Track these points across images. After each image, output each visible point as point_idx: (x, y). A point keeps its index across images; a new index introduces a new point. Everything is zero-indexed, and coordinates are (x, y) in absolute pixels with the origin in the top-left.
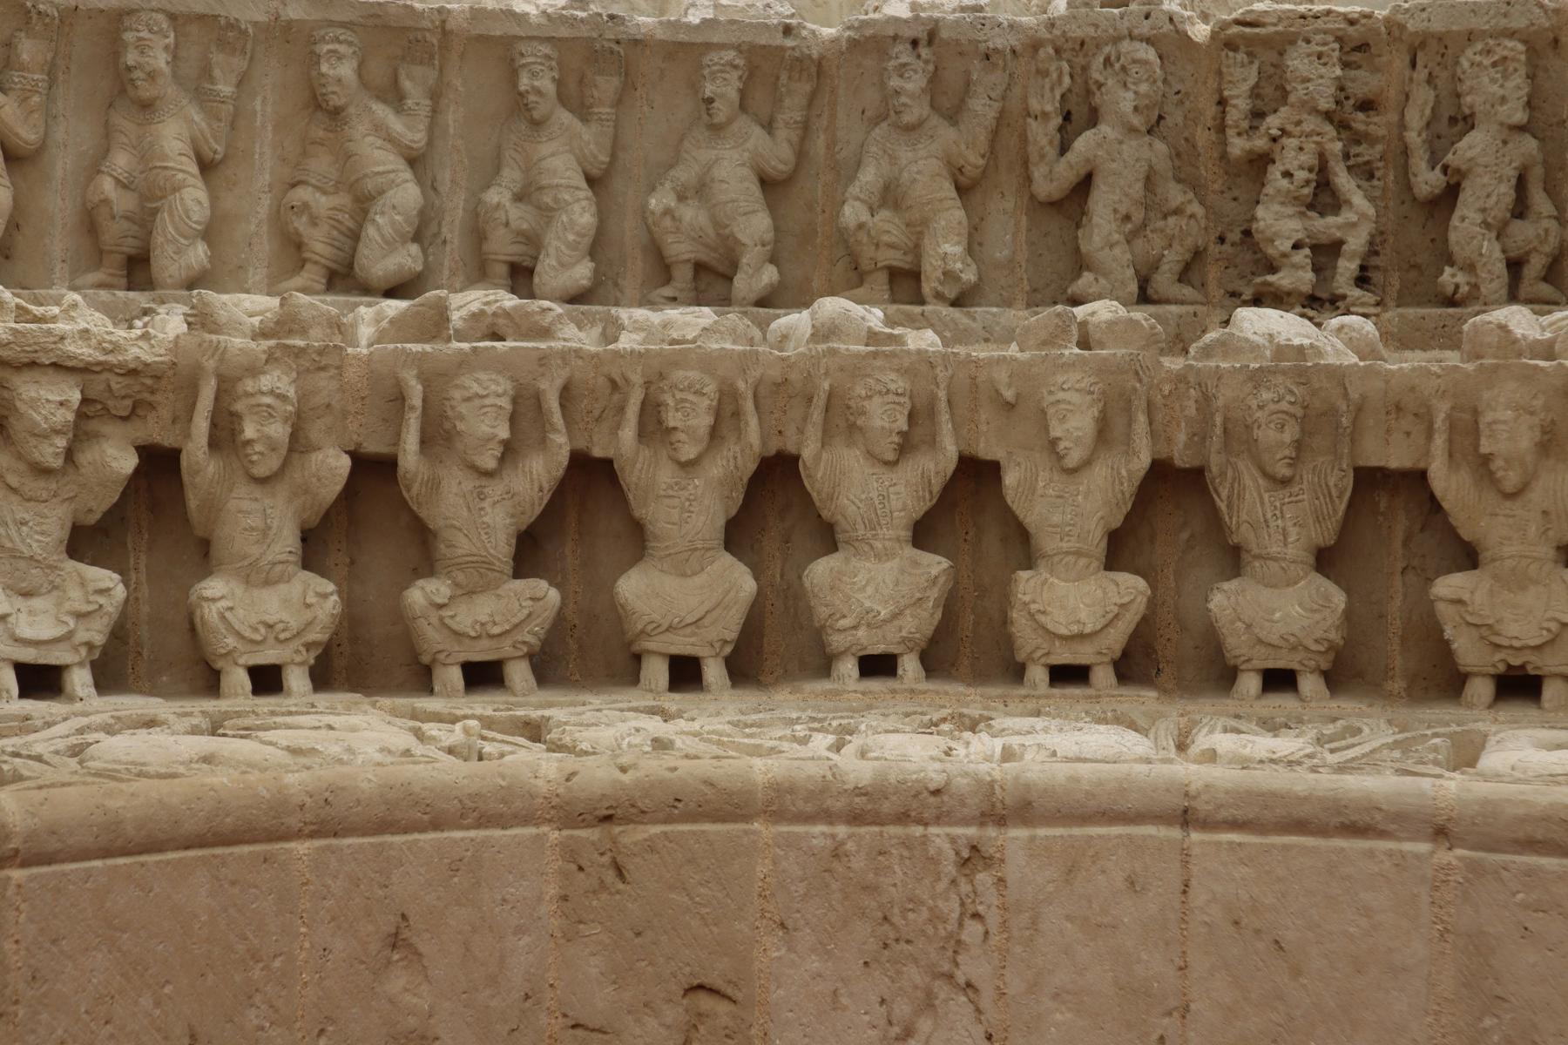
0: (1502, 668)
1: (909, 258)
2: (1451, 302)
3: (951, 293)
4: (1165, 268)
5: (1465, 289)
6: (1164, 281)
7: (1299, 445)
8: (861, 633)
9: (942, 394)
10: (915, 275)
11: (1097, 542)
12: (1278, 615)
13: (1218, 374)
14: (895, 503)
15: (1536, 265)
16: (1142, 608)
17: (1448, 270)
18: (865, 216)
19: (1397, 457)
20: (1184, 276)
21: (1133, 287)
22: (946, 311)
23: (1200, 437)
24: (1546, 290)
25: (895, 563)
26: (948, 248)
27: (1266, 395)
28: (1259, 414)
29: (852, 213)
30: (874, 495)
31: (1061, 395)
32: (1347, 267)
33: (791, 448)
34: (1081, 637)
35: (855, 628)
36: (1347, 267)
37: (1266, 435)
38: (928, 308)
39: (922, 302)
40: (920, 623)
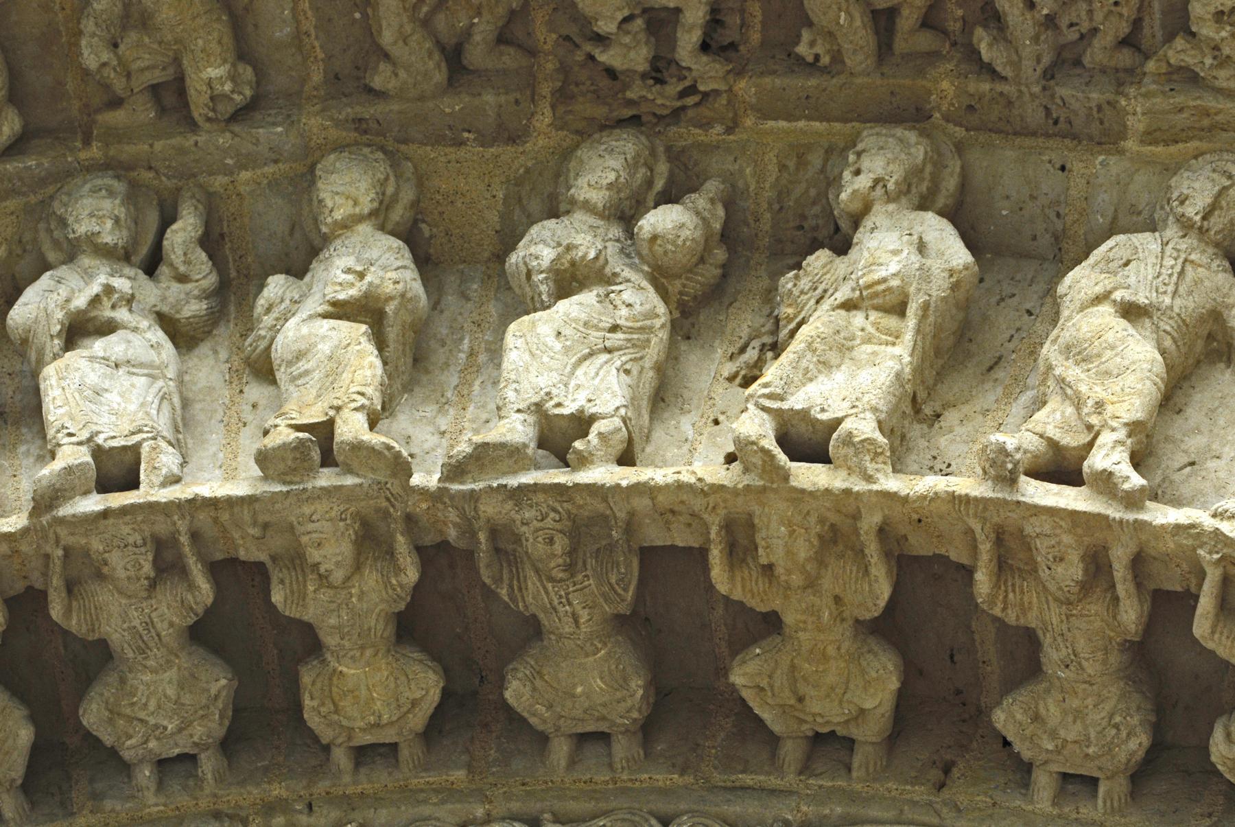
0: (810, 734)
1: (171, 70)
2: (813, 66)
3: (226, 109)
4: (478, 38)
5: (825, 60)
6: (476, 55)
7: (572, 552)
8: (152, 744)
9: (184, 539)
10: (179, 85)
11: (380, 628)
12: (579, 690)
13: (473, 496)
14: (162, 627)
15: (908, 20)
16: (437, 698)
17: (806, 35)
18: (105, 56)
19: (681, 538)
20: (503, 39)
21: (440, 77)
22: (224, 140)
23: (469, 531)
24: (925, 41)
25: (172, 674)
26: (213, 72)
27: (528, 514)
28: (524, 529)
29: (92, 55)
30: (136, 623)
31: (311, 526)
32: (687, 41)
33: (38, 585)
34: (377, 725)
35: (146, 742)
36: (687, 41)
37: (536, 547)
38: (202, 138)
39: (193, 126)
40: (208, 728)
